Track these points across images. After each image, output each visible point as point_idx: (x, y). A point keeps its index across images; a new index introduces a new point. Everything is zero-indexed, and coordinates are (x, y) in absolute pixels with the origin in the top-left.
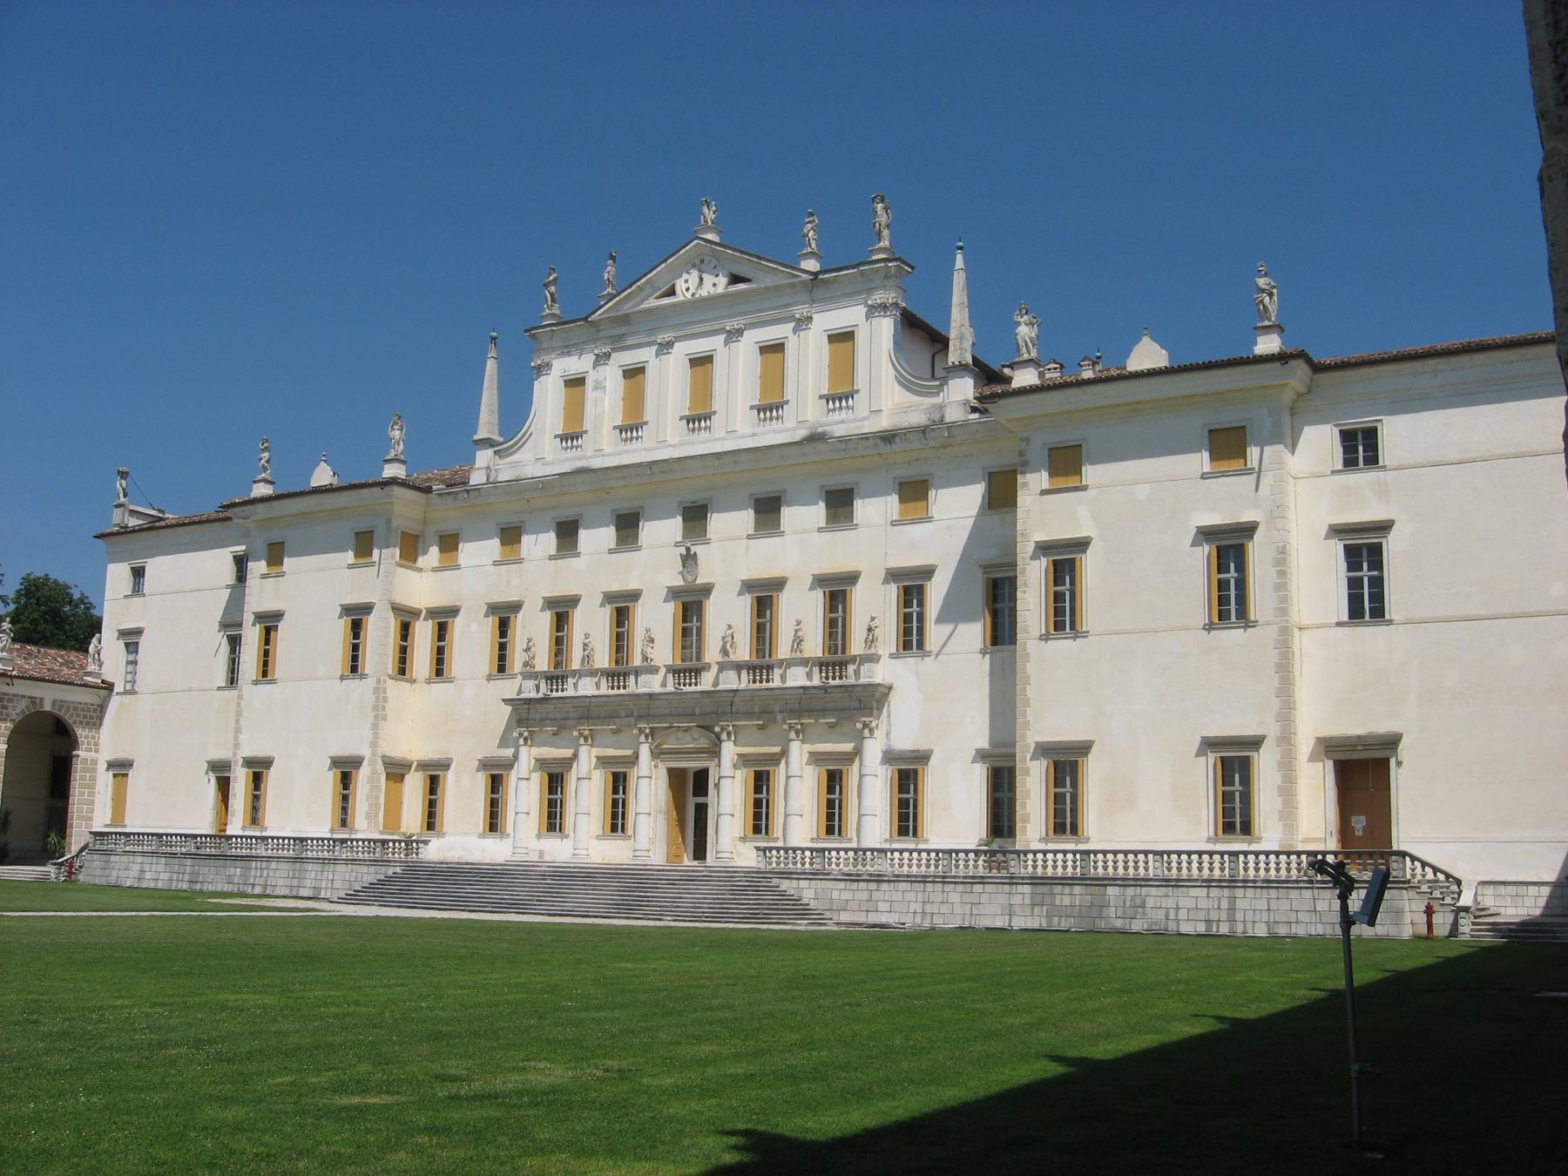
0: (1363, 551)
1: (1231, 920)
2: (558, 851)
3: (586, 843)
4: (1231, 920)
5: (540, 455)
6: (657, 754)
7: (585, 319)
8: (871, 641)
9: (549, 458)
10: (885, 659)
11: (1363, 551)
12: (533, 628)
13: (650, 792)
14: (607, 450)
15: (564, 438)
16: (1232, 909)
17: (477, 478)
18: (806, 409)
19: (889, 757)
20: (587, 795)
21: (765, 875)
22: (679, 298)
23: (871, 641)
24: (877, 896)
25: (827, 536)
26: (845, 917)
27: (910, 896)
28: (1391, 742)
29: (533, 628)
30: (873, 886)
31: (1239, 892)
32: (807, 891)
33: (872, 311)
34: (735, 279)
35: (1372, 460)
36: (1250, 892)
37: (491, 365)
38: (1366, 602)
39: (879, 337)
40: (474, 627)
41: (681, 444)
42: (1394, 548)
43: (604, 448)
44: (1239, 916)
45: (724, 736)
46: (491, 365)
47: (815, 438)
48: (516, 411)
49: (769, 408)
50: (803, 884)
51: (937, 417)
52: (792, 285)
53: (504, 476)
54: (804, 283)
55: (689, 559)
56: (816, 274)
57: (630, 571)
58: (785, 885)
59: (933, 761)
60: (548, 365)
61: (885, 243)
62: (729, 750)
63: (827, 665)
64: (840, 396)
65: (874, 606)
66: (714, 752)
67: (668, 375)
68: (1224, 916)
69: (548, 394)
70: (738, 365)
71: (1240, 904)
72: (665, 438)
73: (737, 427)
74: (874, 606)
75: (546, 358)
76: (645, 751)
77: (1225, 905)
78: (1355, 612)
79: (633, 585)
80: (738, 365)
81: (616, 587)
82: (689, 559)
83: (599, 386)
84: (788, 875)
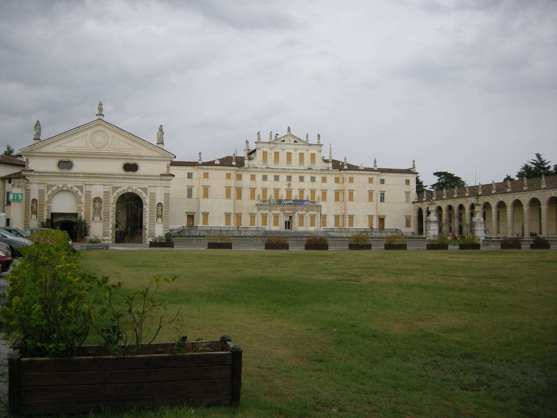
0: (383, 194)
6: (284, 214)
11: (383, 194)
12: (259, 192)
17: (246, 166)
20: (270, 220)
28: (385, 216)
35: (383, 183)
38: (382, 200)
42: (386, 194)
47: (310, 169)
55: (289, 185)
65: (318, 194)
66: (294, 213)
78: (381, 201)
82: (289, 185)
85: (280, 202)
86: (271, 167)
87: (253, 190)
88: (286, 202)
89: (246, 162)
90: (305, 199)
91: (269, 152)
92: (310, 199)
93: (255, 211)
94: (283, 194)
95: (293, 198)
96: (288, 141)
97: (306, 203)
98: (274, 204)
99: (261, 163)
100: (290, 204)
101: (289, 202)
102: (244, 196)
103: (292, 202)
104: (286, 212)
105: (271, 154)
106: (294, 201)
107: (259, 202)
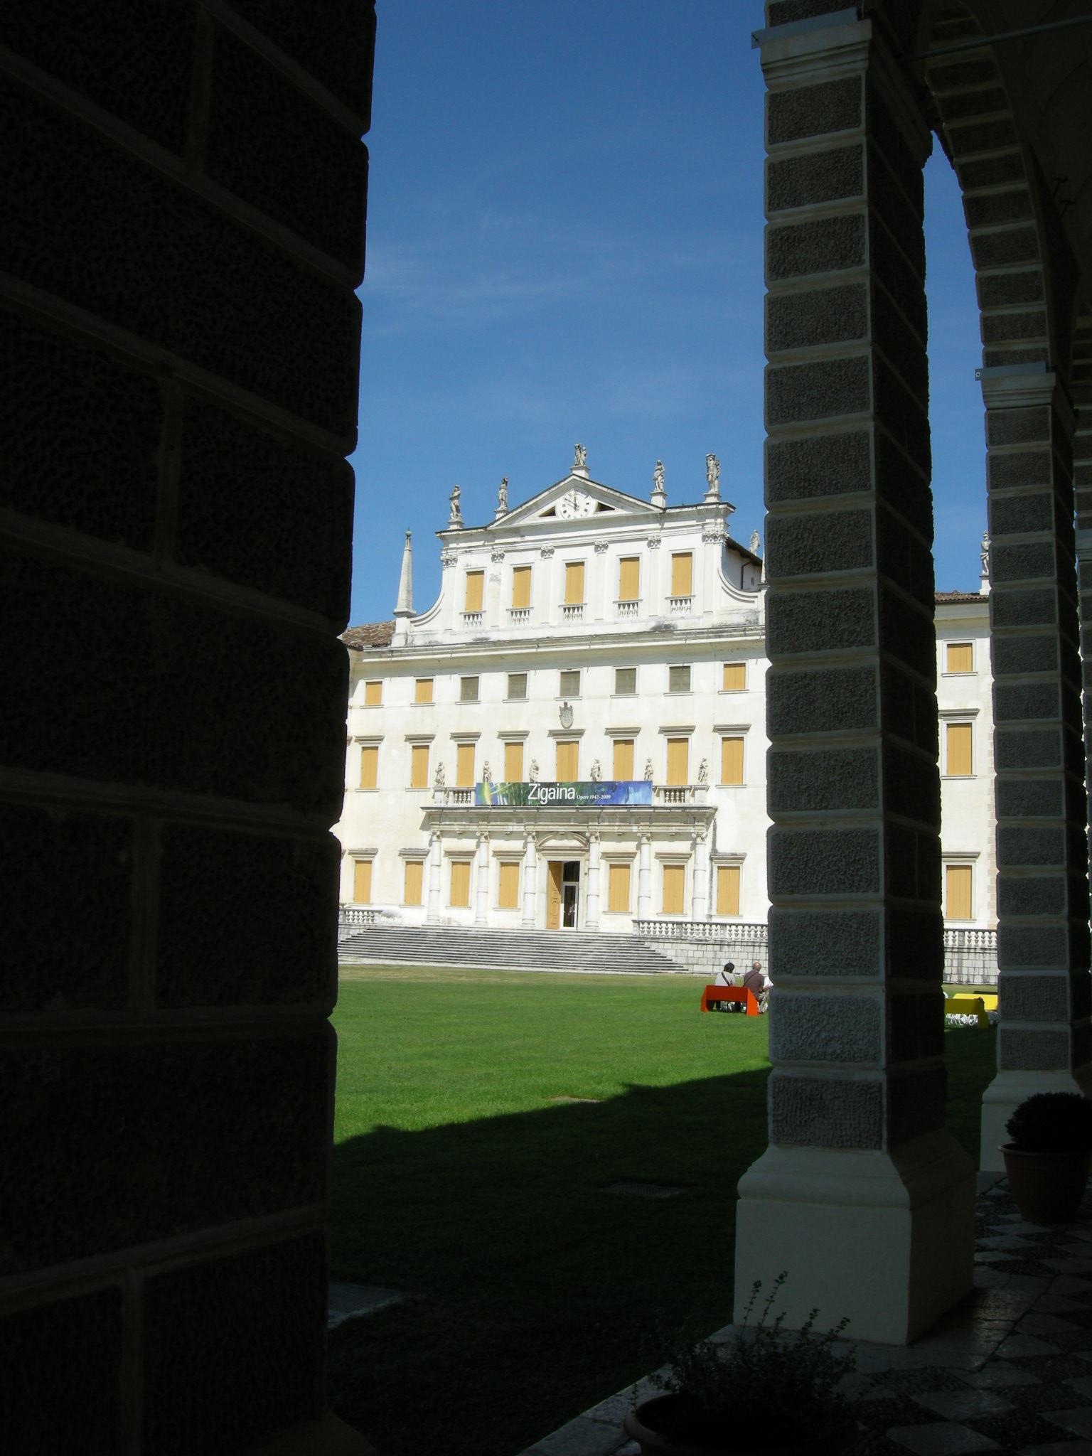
1: (959, 973)
2: (463, 919)
3: (484, 914)
4: (959, 973)
5: (447, 625)
6: (539, 850)
7: (485, 528)
8: (702, 776)
9: (455, 629)
10: (713, 789)
12: (444, 753)
13: (535, 877)
14: (502, 627)
15: (467, 616)
16: (960, 966)
17: (397, 642)
18: (654, 607)
19: (714, 856)
21: (639, 940)
22: (559, 518)
23: (702, 776)
24: (719, 955)
25: (671, 699)
26: (697, 969)
27: (744, 955)
29: (444, 753)
30: (717, 948)
31: (965, 956)
32: (669, 951)
33: (705, 538)
34: (602, 508)
36: (972, 955)
37: (406, 555)
39: (710, 558)
40: (395, 752)
41: (560, 626)
43: (498, 624)
44: (965, 971)
45: (593, 839)
46: (406, 555)
47: (663, 630)
48: (426, 594)
49: (627, 604)
50: (668, 946)
51: (752, 618)
52: (647, 516)
53: (419, 641)
54: (656, 515)
55: (566, 710)
56: (664, 509)
57: (518, 716)
58: (654, 946)
59: (746, 862)
60: (455, 560)
61: (714, 490)
62: (598, 848)
63: (670, 791)
64: (681, 600)
66: (586, 849)
67: (549, 578)
68: (955, 971)
69: (453, 581)
70: (602, 573)
71: (965, 963)
72: (546, 620)
73: (602, 616)
74: (705, 747)
75: (452, 554)
76: (531, 847)
77: (955, 963)
79: (521, 728)
80: (602, 573)
81: (508, 728)
82: (566, 710)
83: (495, 579)
84: (655, 940)
85: (519, 793)
86: (494, 637)
87: (420, 743)
88: (545, 796)
89: (402, 624)
90: (638, 776)
91: (491, 569)
92: (660, 779)
93: (422, 839)
94: (541, 762)
95: (584, 777)
96: (570, 510)
97: (635, 797)
98: (494, 806)
99: (457, 622)
100: (562, 802)
101: (557, 794)
102: (383, 778)
103: (571, 794)
104: (553, 843)
105: (495, 579)
106: (581, 787)
107: (440, 800)
